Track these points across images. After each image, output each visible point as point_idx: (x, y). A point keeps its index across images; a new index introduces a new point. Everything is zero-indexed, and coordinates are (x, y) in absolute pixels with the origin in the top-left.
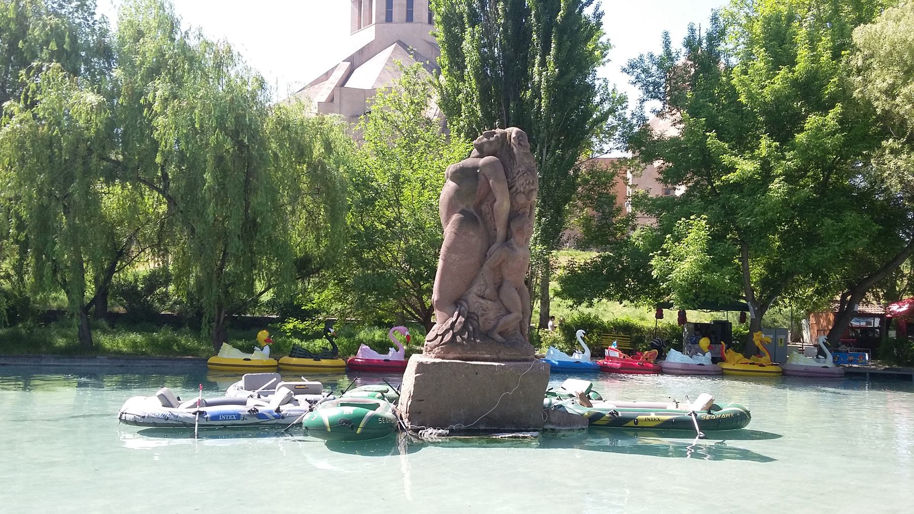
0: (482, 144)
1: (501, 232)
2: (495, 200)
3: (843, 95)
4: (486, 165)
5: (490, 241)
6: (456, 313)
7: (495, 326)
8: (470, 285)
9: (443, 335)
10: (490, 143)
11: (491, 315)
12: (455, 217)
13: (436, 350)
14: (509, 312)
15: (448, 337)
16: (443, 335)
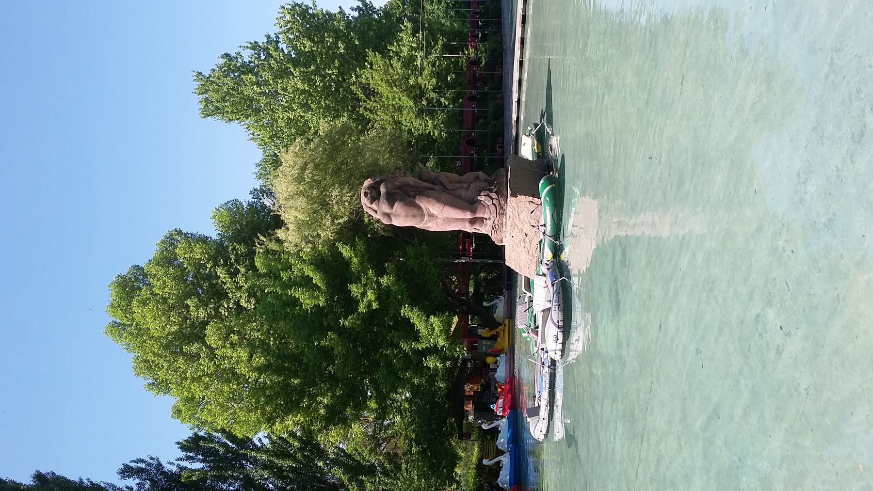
0: (371, 196)
1: (427, 185)
2: (409, 185)
3: (332, 245)
4: (386, 187)
5: (433, 189)
6: (479, 198)
7: (486, 181)
8: (460, 197)
9: (492, 199)
10: (371, 192)
11: (479, 184)
12: (417, 202)
13: (502, 202)
14: (478, 178)
15: (494, 195)
16: (492, 199)
